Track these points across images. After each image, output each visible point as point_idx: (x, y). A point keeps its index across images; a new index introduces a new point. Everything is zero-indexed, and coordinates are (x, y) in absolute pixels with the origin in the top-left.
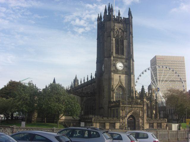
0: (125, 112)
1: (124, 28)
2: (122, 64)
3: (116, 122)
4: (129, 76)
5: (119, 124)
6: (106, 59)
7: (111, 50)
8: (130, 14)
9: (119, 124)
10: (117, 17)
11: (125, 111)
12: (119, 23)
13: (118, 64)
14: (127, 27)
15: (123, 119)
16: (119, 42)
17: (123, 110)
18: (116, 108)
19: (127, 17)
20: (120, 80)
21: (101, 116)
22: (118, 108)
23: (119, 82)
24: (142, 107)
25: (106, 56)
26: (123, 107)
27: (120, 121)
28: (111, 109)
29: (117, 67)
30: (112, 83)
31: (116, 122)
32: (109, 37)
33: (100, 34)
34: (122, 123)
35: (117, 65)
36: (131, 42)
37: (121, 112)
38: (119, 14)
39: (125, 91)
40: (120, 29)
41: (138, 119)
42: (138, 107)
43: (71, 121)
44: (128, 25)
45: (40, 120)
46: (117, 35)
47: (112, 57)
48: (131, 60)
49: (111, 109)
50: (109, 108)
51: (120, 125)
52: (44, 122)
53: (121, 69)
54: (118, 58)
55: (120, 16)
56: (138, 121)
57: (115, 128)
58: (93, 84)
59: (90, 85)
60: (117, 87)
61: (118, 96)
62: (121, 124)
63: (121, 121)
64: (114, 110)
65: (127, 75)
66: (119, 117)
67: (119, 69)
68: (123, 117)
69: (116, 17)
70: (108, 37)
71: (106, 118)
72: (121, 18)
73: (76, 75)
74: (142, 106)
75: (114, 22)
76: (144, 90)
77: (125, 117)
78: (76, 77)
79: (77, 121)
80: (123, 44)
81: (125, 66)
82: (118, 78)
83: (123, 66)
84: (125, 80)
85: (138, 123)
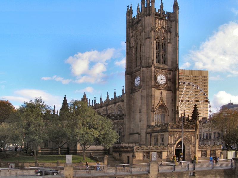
0: (174, 138)
1: (168, 26)
2: (164, 77)
3: (163, 150)
4: (173, 92)
5: (166, 153)
6: (144, 69)
7: (151, 57)
8: (176, 6)
9: (166, 153)
10: (158, 10)
11: (174, 136)
12: (161, 19)
13: (159, 76)
14: (171, 25)
15: (171, 147)
16: (162, 47)
17: (171, 136)
18: (161, 133)
19: (171, 11)
20: (161, 97)
21: (136, 144)
22: (163, 133)
23: (160, 100)
24: (194, 132)
25: (143, 65)
26: (171, 131)
27: (168, 149)
29: (158, 80)
30: (152, 102)
31: (163, 150)
32: (148, 39)
33: (131, 35)
34: (170, 152)
35: (158, 78)
36: (177, 47)
37: (169, 138)
38: (162, 6)
39: (167, 112)
40: (163, 27)
42: (189, 132)
44: (174, 23)
45: (49, 151)
46: (159, 36)
47: (153, 67)
48: (176, 71)
49: (151, 135)
50: (147, 133)
51: (168, 154)
52: (58, 154)
53: (162, 83)
54: (159, 68)
55: (164, 10)
57: (161, 158)
58: (118, 104)
59: (113, 105)
60: (158, 106)
61: (158, 119)
62: (169, 153)
63: (169, 150)
64: (157, 136)
65: (170, 92)
66: (166, 144)
67: (160, 83)
68: (171, 145)
69: (157, 11)
70: (147, 38)
71: (145, 146)
72: (164, 12)
75: (155, 17)
76: (198, 110)
77: (174, 144)
80: (165, 50)
81: (168, 80)
82: (160, 95)
83: (165, 79)
84: (167, 97)
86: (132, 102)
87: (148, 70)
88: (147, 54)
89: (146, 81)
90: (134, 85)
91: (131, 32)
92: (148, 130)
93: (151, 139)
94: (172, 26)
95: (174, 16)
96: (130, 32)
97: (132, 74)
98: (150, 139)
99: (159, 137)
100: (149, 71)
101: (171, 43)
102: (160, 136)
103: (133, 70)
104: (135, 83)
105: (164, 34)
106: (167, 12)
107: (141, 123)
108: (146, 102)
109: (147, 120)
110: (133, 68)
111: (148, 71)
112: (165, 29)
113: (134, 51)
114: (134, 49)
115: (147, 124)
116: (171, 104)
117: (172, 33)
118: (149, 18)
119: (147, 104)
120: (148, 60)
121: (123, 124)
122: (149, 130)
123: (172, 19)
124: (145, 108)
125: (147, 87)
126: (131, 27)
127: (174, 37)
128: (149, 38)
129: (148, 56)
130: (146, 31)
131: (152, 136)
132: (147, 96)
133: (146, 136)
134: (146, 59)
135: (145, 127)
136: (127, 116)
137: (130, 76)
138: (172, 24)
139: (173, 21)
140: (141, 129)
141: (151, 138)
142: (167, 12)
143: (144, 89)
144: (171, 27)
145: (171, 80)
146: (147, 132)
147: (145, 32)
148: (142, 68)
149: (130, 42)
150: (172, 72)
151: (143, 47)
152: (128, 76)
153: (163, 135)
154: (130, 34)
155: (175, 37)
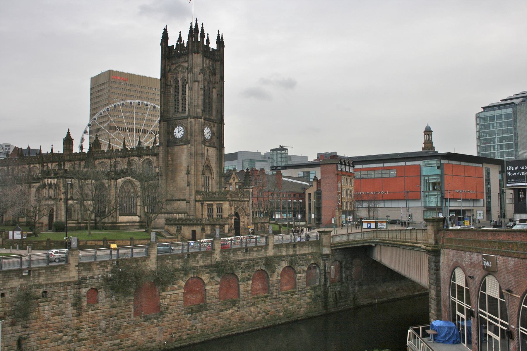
14: (216, 66)
18: (218, 202)
22: (221, 202)
28: (202, 204)
32: (197, 83)
39: (212, 173)
41: (243, 219)
43: (129, 224)
44: (219, 63)
48: (222, 124)
49: (202, 204)
55: (210, 46)
56: (243, 220)
64: (212, 204)
70: (195, 81)
72: (210, 48)
73: (69, 130)
74: (248, 199)
78: (69, 133)
79: (137, 224)
81: (213, 134)
85: (243, 224)
86: (169, 158)
87: (195, 121)
88: (195, 101)
89: (194, 135)
90: (173, 136)
91: (168, 65)
92: (197, 197)
93: (203, 209)
94: (217, 67)
95: (219, 54)
96: (167, 65)
97: (170, 120)
98: (200, 209)
99: (215, 207)
100: (197, 122)
101: (216, 88)
102: (216, 205)
103: (171, 115)
104: (175, 134)
105: (209, 76)
106: (212, 48)
107: (190, 188)
108: (194, 161)
109: (195, 184)
110: (171, 113)
111: (196, 123)
112: (211, 70)
113: (172, 91)
114: (172, 89)
115: (195, 189)
116: (216, 164)
117: (217, 76)
118: (198, 56)
119: (195, 164)
120: (196, 109)
121: (157, 186)
122: (199, 197)
123: (216, 57)
124: (193, 169)
125: (196, 142)
126: (168, 58)
127: (219, 80)
128: (198, 81)
129: (196, 105)
130: (194, 72)
131: (204, 205)
132: (195, 153)
133: (195, 205)
134: (194, 107)
135: (193, 192)
136: (163, 176)
137: (166, 123)
138: (217, 65)
139: (218, 61)
140: (190, 195)
141: (202, 207)
142: (212, 48)
143: (192, 145)
144: (216, 68)
145: (216, 134)
146: (196, 199)
147: (193, 74)
148: (191, 118)
149: (166, 78)
150: (216, 124)
151: (191, 92)
152: (164, 123)
153: (221, 204)
154: (166, 67)
155: (220, 81)
